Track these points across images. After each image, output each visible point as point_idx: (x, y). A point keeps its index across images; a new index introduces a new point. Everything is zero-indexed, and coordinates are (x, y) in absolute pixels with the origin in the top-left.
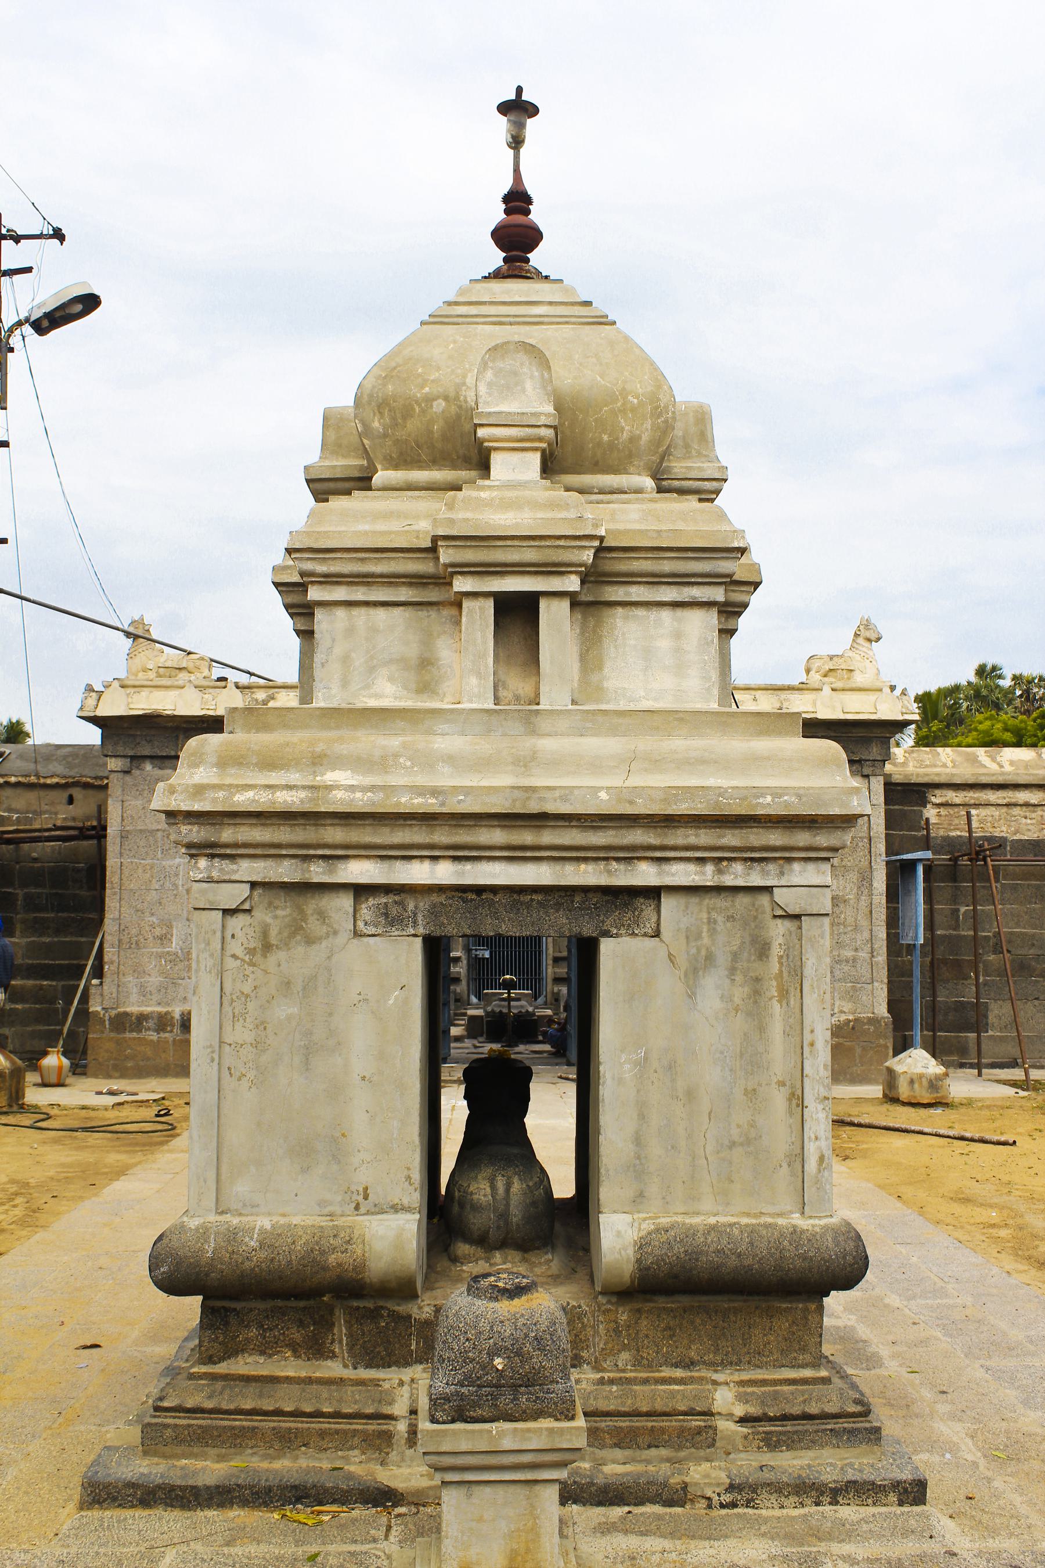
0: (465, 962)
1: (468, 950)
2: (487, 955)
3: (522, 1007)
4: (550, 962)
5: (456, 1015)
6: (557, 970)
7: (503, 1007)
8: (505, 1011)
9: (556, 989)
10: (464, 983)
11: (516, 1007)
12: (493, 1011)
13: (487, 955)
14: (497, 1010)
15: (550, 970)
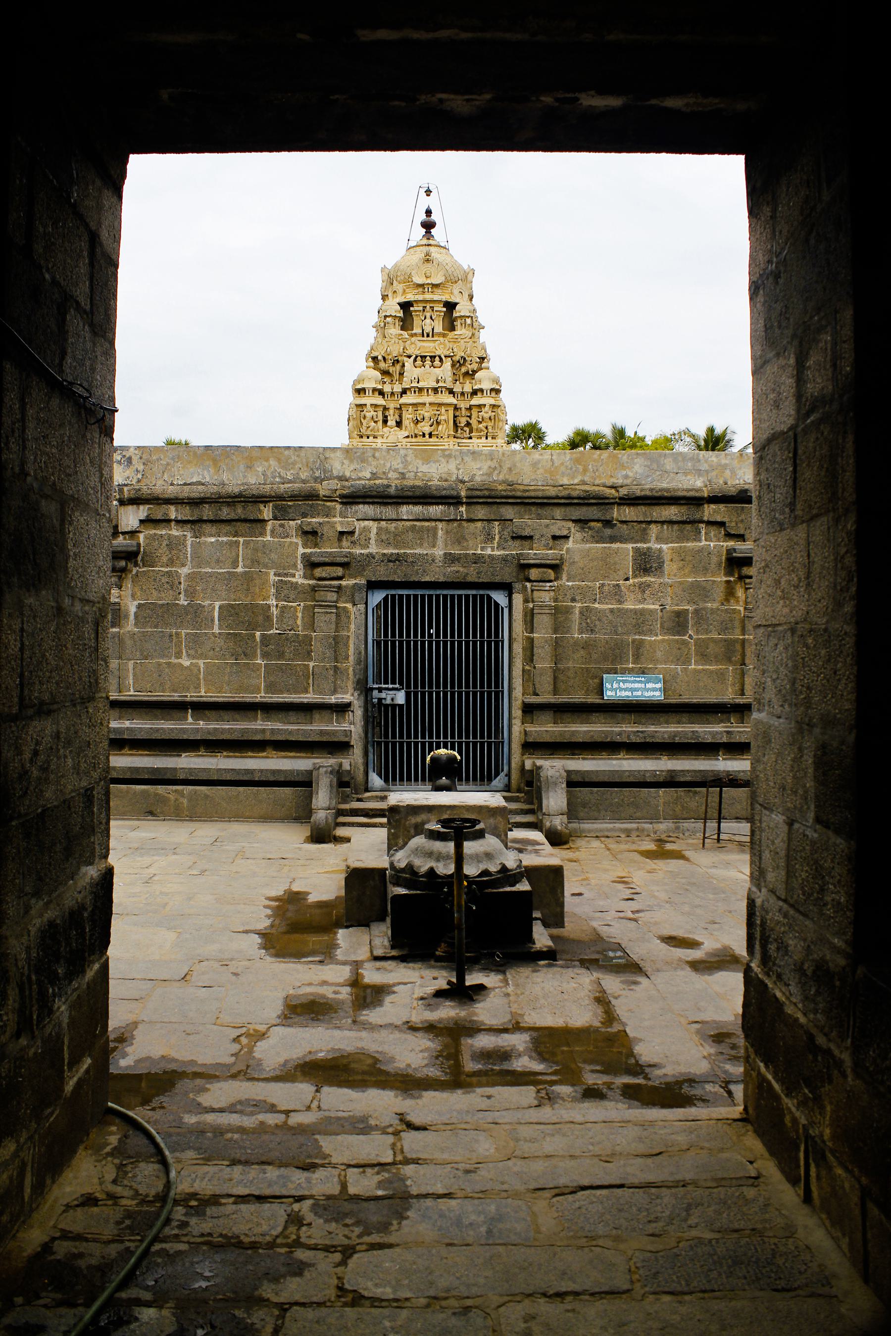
0: (359, 713)
1: (365, 690)
2: (400, 698)
3: (489, 856)
4: (517, 713)
5: (341, 813)
6: (530, 728)
7: (439, 857)
8: (446, 869)
9: (528, 765)
10: (357, 751)
11: (477, 858)
12: (410, 868)
13: (400, 698)
14: (423, 865)
15: (517, 728)
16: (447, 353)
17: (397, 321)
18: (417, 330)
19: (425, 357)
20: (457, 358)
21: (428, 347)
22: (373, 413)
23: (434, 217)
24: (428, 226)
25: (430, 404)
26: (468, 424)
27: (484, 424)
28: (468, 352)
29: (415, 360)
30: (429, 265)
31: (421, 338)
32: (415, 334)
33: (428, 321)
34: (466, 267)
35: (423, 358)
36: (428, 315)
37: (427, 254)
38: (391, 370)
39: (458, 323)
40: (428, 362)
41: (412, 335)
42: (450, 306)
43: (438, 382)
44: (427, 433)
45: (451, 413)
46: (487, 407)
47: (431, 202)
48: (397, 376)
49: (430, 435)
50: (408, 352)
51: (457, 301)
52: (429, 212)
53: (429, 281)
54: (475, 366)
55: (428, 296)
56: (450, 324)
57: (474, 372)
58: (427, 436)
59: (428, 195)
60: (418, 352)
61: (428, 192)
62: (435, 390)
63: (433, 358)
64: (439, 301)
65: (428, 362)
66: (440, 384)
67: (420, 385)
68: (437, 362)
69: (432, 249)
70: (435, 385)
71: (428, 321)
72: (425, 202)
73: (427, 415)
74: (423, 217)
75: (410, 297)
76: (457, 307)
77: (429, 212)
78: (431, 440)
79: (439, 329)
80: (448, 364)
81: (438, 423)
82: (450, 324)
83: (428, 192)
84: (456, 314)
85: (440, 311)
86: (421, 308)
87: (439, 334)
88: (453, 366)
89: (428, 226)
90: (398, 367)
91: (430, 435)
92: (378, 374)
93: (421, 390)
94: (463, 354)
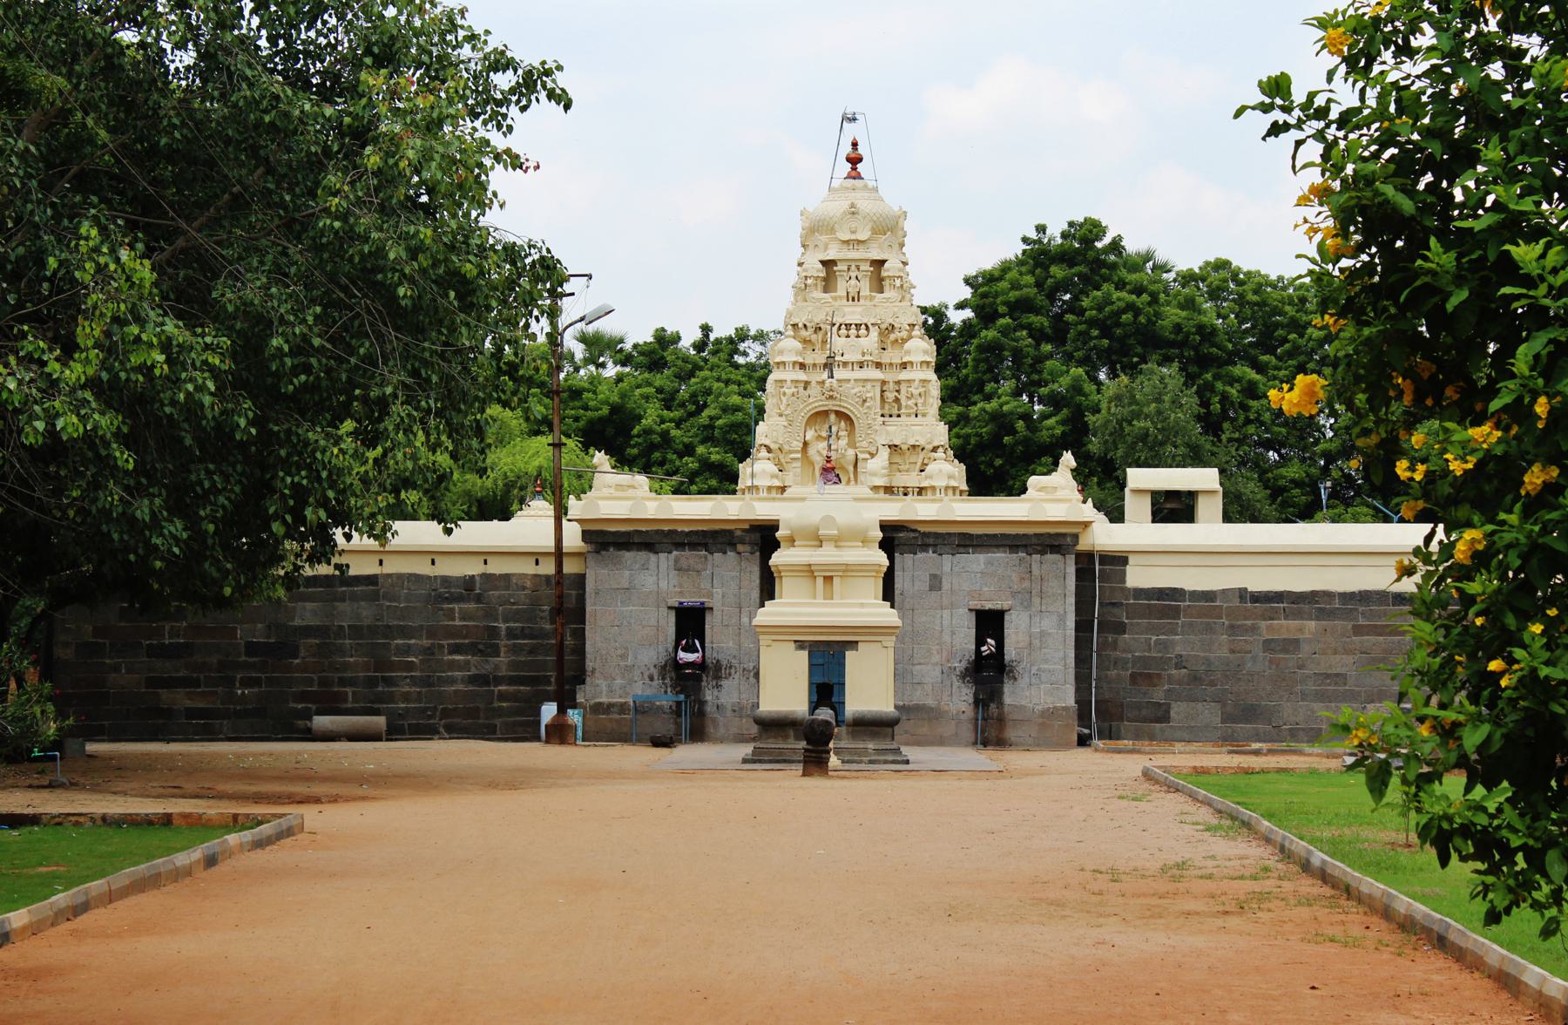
18: (841, 292)
20: (883, 326)
21: (853, 314)
23: (861, 150)
24: (855, 160)
26: (897, 400)
33: (853, 281)
35: (848, 326)
36: (853, 275)
37: (853, 206)
38: (814, 337)
39: (886, 283)
40: (853, 331)
41: (835, 299)
48: (818, 346)
52: (855, 145)
54: (904, 334)
56: (879, 284)
57: (904, 341)
63: (858, 326)
65: (853, 331)
66: (867, 358)
68: (863, 331)
69: (859, 194)
70: (859, 358)
71: (853, 281)
74: (849, 149)
75: (831, 255)
77: (855, 145)
79: (865, 292)
80: (874, 333)
82: (879, 284)
84: (884, 274)
88: (880, 334)
89: (855, 160)
90: (820, 334)
92: (799, 346)
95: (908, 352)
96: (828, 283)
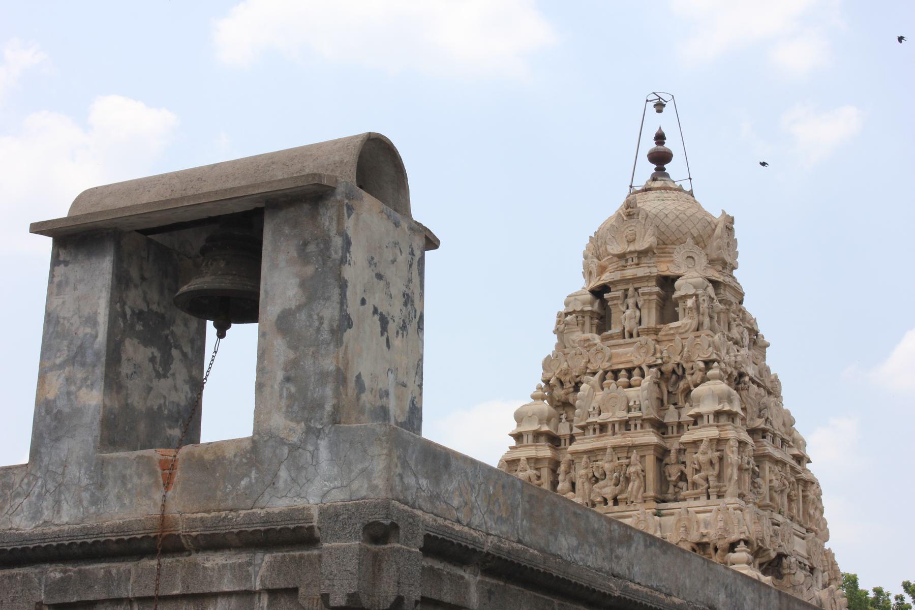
16: (651, 360)
17: (587, 319)
18: (615, 329)
19: (619, 370)
21: (629, 354)
22: (531, 472)
23: (668, 145)
24: (660, 158)
25: (614, 448)
26: (683, 477)
27: (703, 474)
28: (685, 353)
29: (603, 379)
30: (632, 222)
31: (622, 341)
32: (611, 337)
34: (717, 214)
35: (616, 373)
40: (623, 379)
42: (667, 282)
43: (629, 410)
44: (609, 497)
45: (650, 460)
46: (702, 447)
47: (665, 122)
49: (616, 502)
50: (591, 367)
51: (678, 272)
52: (660, 138)
53: (632, 248)
55: (629, 273)
58: (610, 503)
59: (659, 111)
60: (606, 365)
61: (660, 107)
62: (626, 424)
63: (630, 371)
64: (647, 278)
67: (604, 417)
68: (636, 378)
70: (622, 415)
72: (655, 122)
73: (607, 466)
74: (652, 145)
76: (677, 283)
77: (660, 138)
78: (616, 508)
79: (650, 319)
81: (628, 480)
83: (660, 107)
85: (650, 294)
86: (620, 293)
87: (648, 331)
89: (660, 158)
91: (616, 502)
93: (603, 427)
94: (678, 359)
95: (699, 401)
96: (602, 320)
